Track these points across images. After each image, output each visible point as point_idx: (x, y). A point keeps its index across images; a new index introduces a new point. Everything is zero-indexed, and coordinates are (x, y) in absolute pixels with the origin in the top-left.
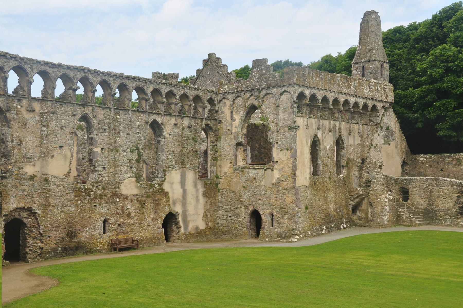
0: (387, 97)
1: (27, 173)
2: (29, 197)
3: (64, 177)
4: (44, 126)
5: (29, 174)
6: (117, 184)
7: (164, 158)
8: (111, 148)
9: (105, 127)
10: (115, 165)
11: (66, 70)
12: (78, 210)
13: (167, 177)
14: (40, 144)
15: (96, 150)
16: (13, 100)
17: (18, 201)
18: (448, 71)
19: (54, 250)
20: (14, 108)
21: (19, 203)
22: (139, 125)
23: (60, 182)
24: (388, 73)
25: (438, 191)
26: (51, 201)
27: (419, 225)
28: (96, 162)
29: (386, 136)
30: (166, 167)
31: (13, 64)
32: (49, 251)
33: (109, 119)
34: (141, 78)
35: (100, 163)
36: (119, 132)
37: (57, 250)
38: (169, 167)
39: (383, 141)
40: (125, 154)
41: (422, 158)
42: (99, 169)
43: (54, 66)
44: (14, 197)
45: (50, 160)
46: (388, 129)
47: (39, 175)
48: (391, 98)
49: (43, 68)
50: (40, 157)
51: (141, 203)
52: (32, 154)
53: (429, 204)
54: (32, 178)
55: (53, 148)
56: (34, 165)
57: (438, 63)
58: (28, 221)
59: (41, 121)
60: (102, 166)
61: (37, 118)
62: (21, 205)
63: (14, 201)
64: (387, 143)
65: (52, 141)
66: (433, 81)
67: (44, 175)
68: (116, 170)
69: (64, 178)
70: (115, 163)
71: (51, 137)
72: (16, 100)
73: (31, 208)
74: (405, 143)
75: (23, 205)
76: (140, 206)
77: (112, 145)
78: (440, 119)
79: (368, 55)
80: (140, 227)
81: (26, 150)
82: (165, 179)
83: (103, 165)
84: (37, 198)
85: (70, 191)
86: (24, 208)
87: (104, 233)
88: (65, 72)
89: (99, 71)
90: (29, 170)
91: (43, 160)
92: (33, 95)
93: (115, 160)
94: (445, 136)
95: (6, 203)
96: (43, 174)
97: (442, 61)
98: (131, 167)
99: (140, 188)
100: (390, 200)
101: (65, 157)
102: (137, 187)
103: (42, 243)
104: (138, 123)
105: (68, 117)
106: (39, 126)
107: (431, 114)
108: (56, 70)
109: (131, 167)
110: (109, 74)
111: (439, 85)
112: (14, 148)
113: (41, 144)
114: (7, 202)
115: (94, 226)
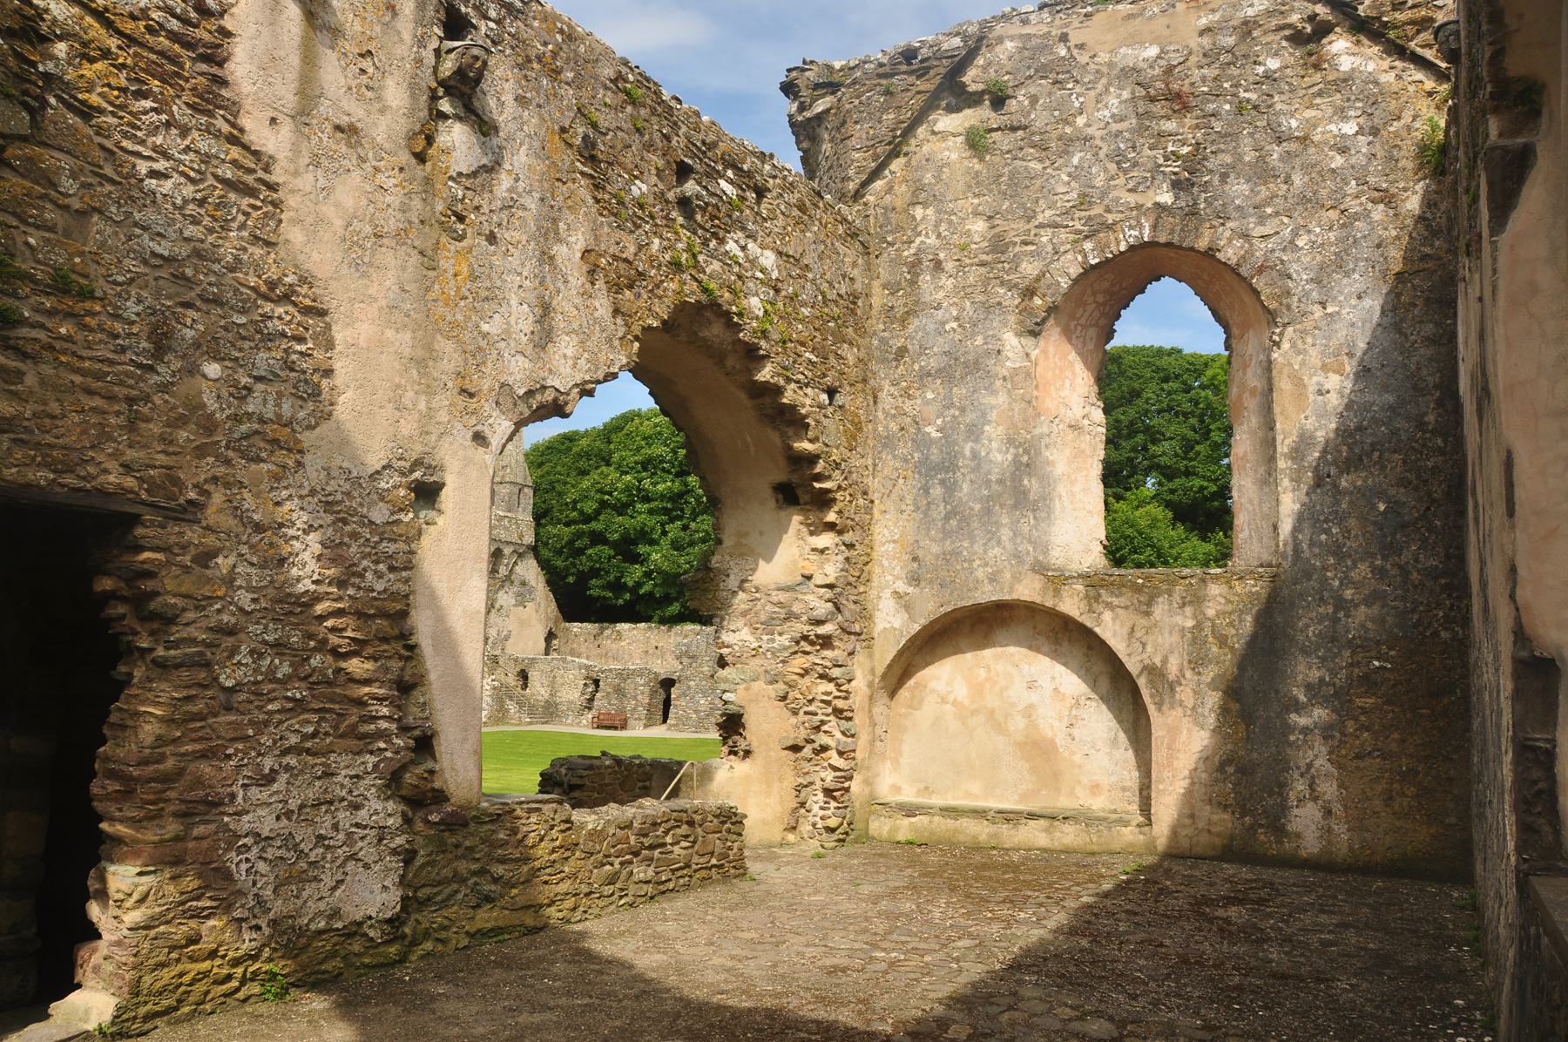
0: (521, 537)
18: (603, 505)
24: (532, 501)
25: (562, 677)
27: (531, 723)
29: (519, 595)
39: (513, 602)
41: (576, 627)
46: (524, 584)
48: (529, 539)
53: (551, 695)
57: (592, 494)
64: (521, 603)
66: (587, 519)
74: (553, 605)
78: (595, 573)
79: (501, 473)
94: (599, 597)
97: (601, 491)
100: (494, 688)
107: (584, 564)
111: (594, 525)
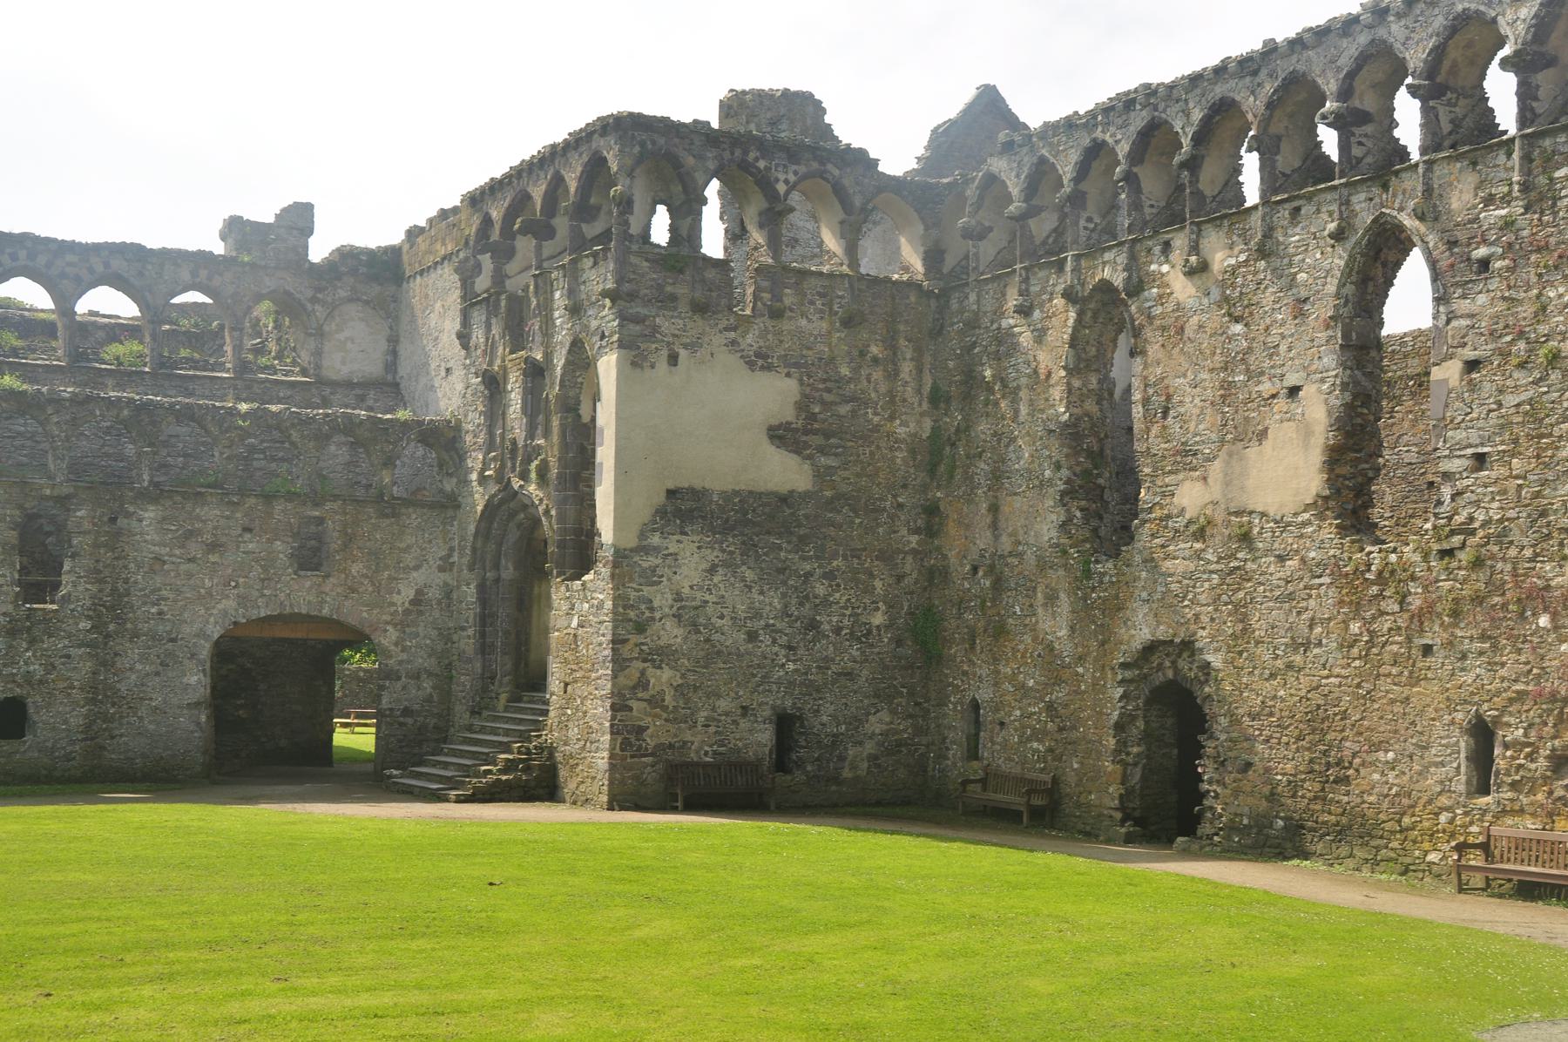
1: (1182, 511)
2: (1186, 603)
3: (1306, 516)
4: (1237, 320)
9: (1482, 252)
10: (1542, 436)
11: (1294, 58)
12: (1349, 665)
14: (1222, 392)
16: (1149, 250)
17: (1156, 616)
21: (1159, 623)
31: (1138, 123)
32: (1245, 821)
37: (1271, 826)
44: (1144, 601)
45: (1252, 452)
47: (1219, 516)
50: (1222, 441)
52: (1197, 439)
55: (1264, 400)
56: (1205, 479)
59: (1227, 299)
60: (1470, 451)
63: (1145, 615)
65: (1262, 373)
67: (1238, 513)
69: (1304, 524)
72: (1157, 249)
73: (1193, 642)
75: (1171, 631)
77: (1521, 334)
83: (1470, 446)
84: (1208, 605)
85: (1320, 576)
86: (1172, 641)
88: (1291, 69)
90: (1190, 497)
91: (1230, 455)
95: (1125, 623)
96: (1230, 514)
105: (1318, 256)
114: (1128, 619)
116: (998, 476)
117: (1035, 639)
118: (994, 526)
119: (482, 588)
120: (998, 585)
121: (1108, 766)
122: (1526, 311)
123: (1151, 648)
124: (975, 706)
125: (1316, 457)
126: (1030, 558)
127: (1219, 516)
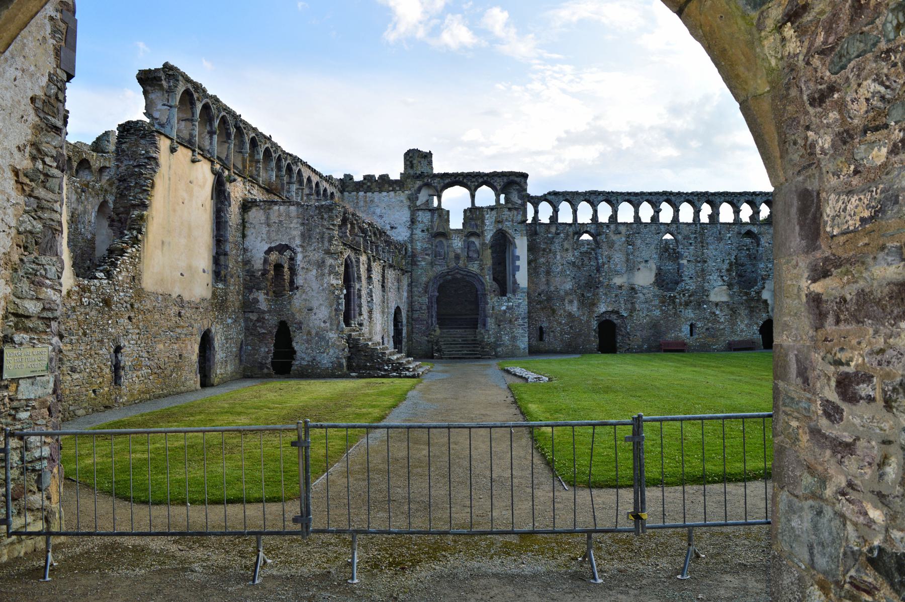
5: (617, 284)
6: (705, 292)
7: (762, 266)
8: (699, 259)
13: (766, 285)
15: (681, 262)
19: (640, 347)
20: (604, 232)
21: (608, 307)
22: (730, 237)
23: (645, 291)
26: (637, 306)
28: (682, 272)
30: (765, 275)
33: (695, 233)
34: (701, 193)
35: (687, 273)
36: (707, 244)
38: (769, 275)
40: (714, 264)
42: (686, 278)
43: (636, 194)
45: (636, 273)
49: (627, 197)
51: (731, 309)
54: (620, 287)
58: (619, 322)
61: (624, 239)
62: (610, 309)
68: (704, 280)
70: (703, 274)
71: (636, 253)
76: (730, 312)
77: (698, 257)
80: (732, 332)
81: (614, 265)
82: (764, 288)
87: (691, 335)
89: (683, 193)
90: (618, 281)
92: (619, 220)
93: (703, 270)
98: (722, 276)
99: (731, 296)
101: (651, 269)
102: (729, 295)
103: (630, 340)
104: (728, 235)
106: (625, 245)
108: (639, 197)
109: (722, 276)
110: (692, 193)
112: (604, 264)
113: (628, 260)
115: (680, 329)
116: (548, 273)
117: (565, 311)
118: (547, 284)
119: (428, 298)
120: (549, 299)
121: (593, 339)
122: (700, 253)
123: (604, 313)
124: (541, 328)
125: (653, 275)
126: (562, 293)
127: (626, 285)
